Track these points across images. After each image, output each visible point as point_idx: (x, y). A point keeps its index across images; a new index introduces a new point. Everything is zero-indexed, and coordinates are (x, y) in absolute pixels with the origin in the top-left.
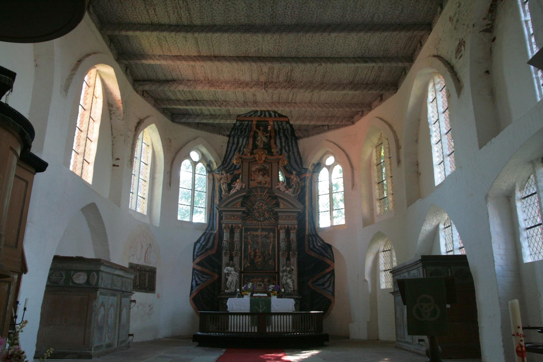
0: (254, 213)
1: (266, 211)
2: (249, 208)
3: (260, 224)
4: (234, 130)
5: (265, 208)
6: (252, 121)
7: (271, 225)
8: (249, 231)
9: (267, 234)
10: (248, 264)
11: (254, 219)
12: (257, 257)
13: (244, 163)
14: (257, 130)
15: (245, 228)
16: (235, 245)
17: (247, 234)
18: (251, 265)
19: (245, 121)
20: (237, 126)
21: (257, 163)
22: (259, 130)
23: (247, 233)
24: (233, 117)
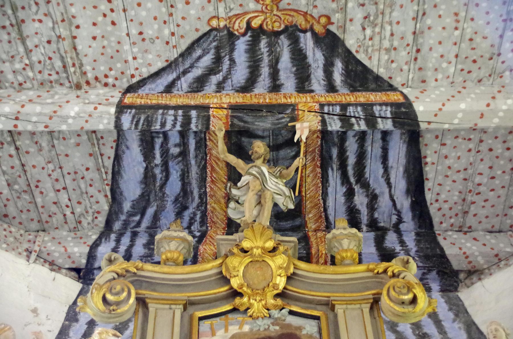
4: (113, 236)
6: (204, 108)
13: (152, 307)
14: (233, 159)
19: (166, 107)
20: (127, 206)
21: (235, 310)
22: (247, 158)
24: (98, 95)
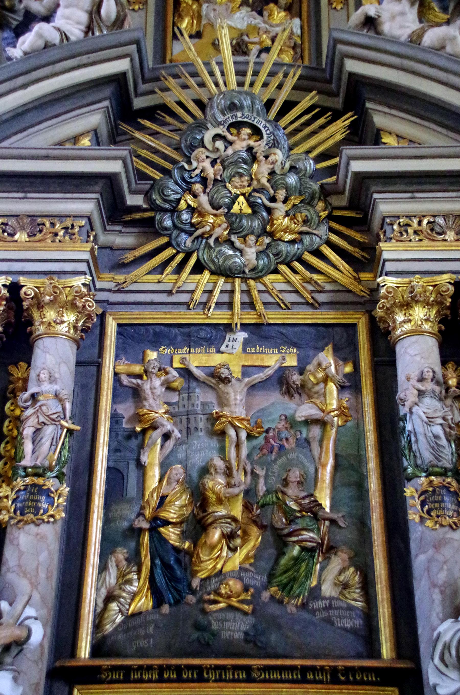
0: (191, 210)
1: (281, 194)
2: (157, 175)
3: (237, 297)
5: (272, 173)
7: (321, 298)
8: (155, 346)
9: (292, 361)
10: (134, 595)
11: (192, 261)
12: (216, 535)
15: (119, 325)
16: (28, 431)
17: (138, 369)
18: (158, 603)
23: (142, 361)
